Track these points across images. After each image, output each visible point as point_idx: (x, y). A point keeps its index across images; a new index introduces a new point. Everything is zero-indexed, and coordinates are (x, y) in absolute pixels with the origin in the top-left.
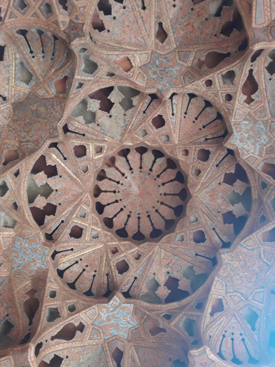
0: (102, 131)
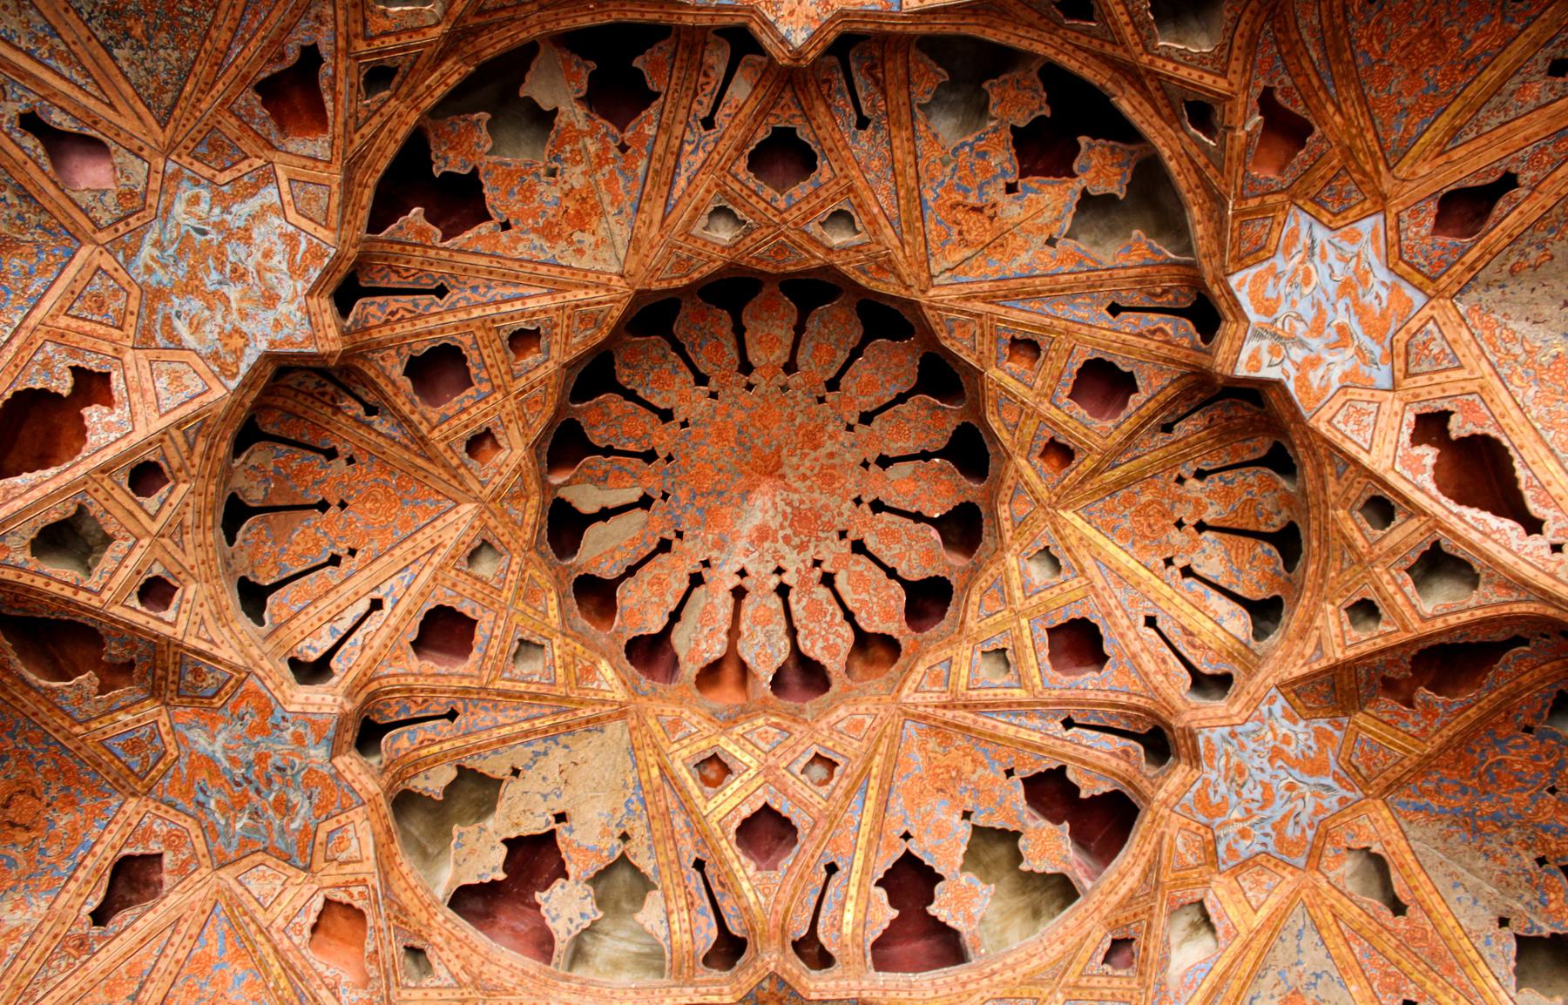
0: (637, 806)
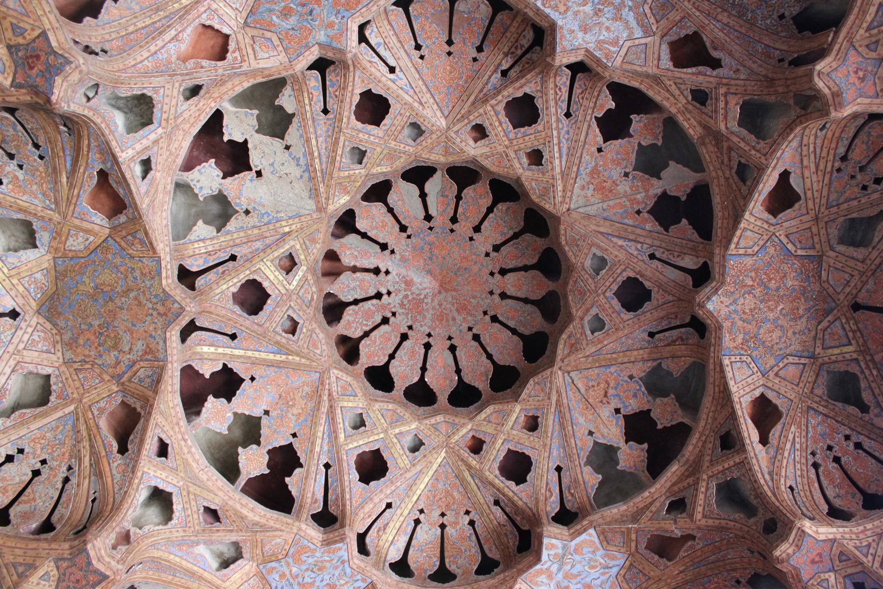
0: (266, 220)
